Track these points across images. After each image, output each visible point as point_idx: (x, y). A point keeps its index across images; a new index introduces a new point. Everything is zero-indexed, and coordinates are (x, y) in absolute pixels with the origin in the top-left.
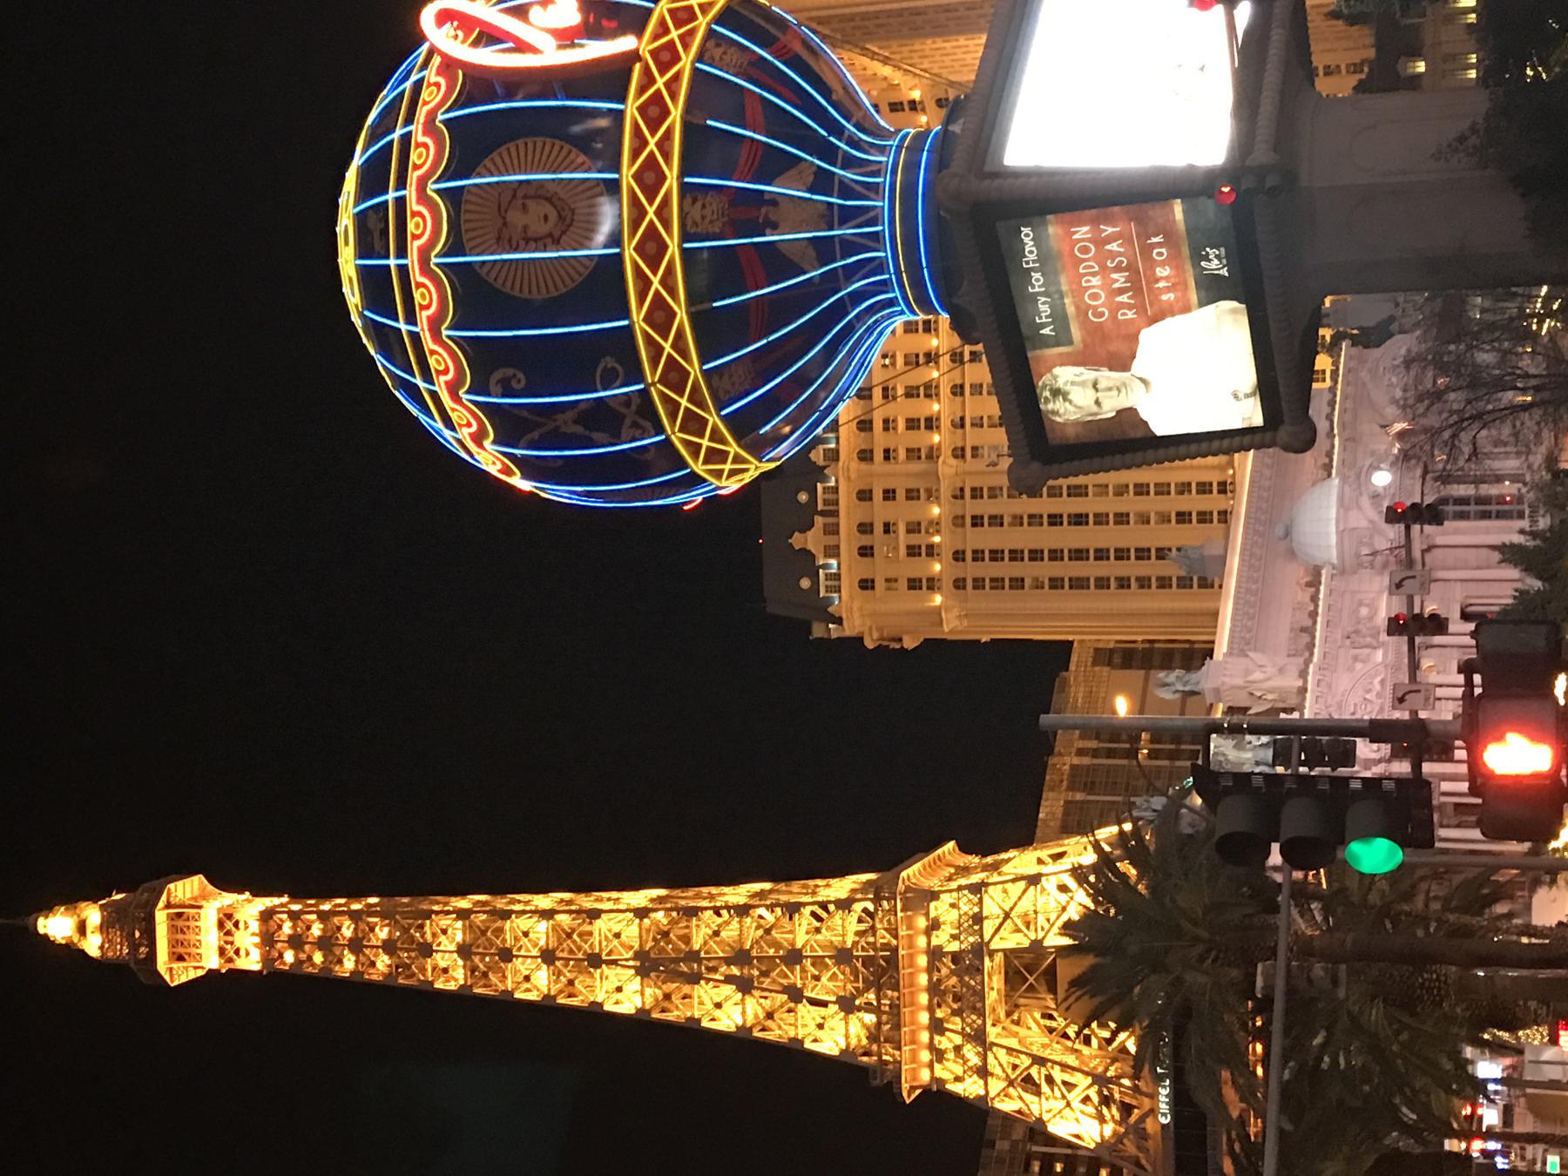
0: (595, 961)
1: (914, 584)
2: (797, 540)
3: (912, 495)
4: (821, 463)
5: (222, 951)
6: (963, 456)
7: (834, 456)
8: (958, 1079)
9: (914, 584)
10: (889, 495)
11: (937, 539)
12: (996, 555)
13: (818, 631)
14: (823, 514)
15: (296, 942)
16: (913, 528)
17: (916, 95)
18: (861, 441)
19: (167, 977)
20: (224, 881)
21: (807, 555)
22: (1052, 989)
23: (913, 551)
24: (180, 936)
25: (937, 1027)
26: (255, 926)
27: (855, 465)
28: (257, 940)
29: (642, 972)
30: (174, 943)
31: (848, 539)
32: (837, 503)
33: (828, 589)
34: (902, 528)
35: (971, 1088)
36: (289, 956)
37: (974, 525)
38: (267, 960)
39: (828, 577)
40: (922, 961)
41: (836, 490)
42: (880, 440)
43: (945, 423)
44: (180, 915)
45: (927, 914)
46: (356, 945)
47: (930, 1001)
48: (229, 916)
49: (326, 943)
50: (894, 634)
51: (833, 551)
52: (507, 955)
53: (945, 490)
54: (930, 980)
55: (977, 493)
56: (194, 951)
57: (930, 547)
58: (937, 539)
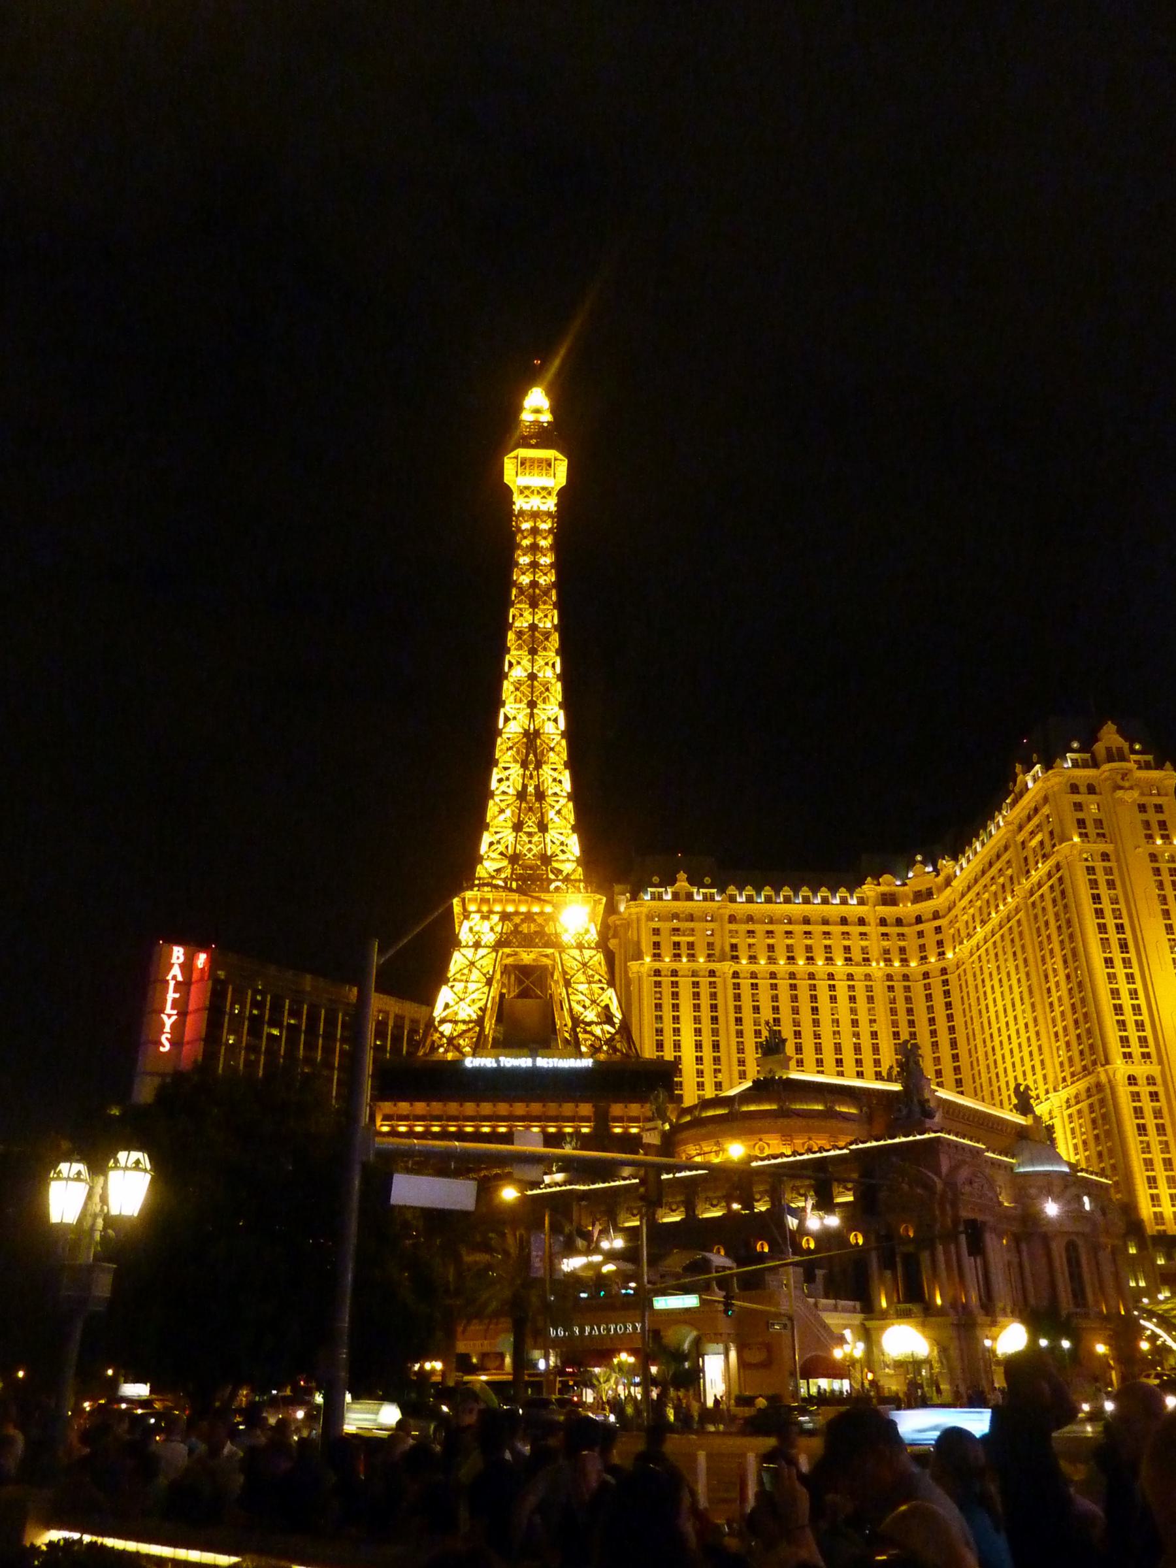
0: (532, 705)
1: (657, 945)
2: (682, 876)
5: (527, 488)
6: (734, 977)
7: (732, 899)
8: (471, 929)
9: (657, 945)
11: (684, 959)
12: (675, 995)
13: (617, 888)
15: (535, 531)
16: (691, 945)
17: (949, 955)
19: (512, 454)
20: (562, 493)
21: (673, 882)
22: (519, 996)
23: (677, 945)
25: (505, 917)
26: (544, 508)
28: (535, 509)
29: (526, 733)
30: (532, 460)
31: (682, 906)
33: (653, 894)
34: (690, 939)
35: (465, 936)
36: (526, 526)
37: (693, 983)
38: (522, 513)
39: (660, 894)
41: (713, 900)
43: (753, 968)
44: (550, 465)
46: (534, 565)
47: (522, 913)
48: (549, 493)
49: (534, 548)
50: (621, 931)
51: (676, 897)
52: (533, 652)
54: (536, 914)
55: (712, 984)
56: (527, 471)
57: (679, 955)
58: (684, 959)
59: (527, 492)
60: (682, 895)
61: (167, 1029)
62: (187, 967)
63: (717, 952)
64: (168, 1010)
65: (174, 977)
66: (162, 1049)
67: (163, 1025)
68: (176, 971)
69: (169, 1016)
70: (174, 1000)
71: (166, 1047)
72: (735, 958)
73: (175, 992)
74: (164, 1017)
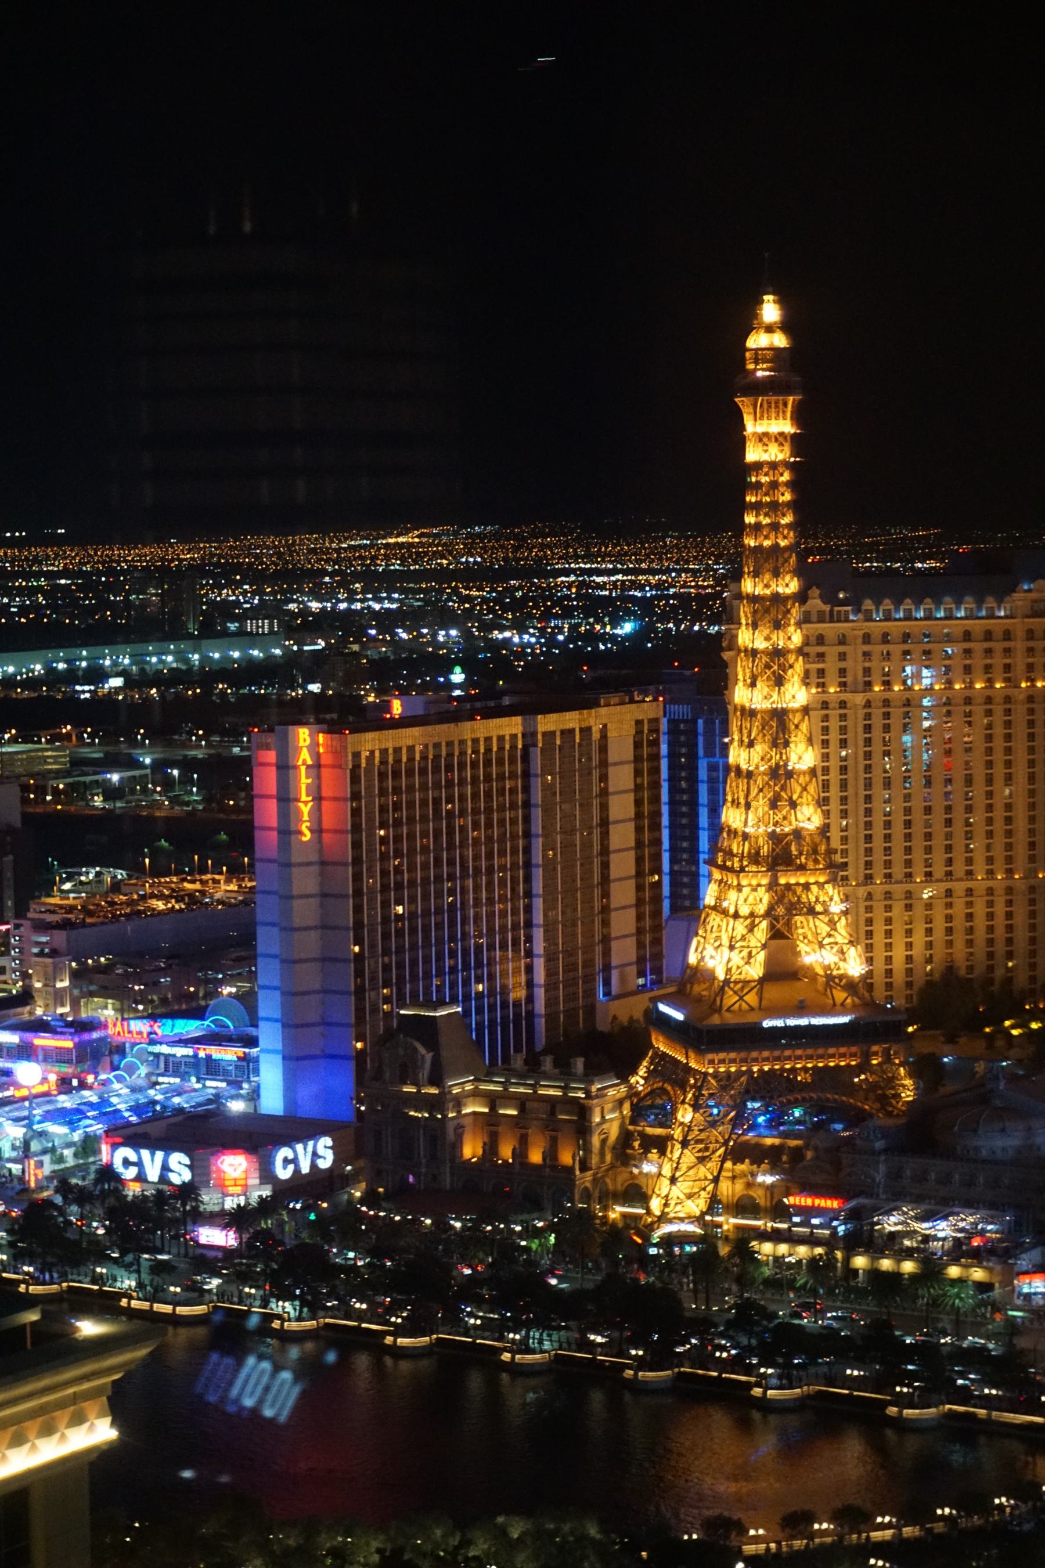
3: (843, 672)
4: (864, 608)
5: (766, 434)
10: (842, 657)
14: (831, 611)
18: (876, 635)
24: (773, 405)
27: (861, 633)
32: (839, 621)
34: (821, 666)
40: (802, 881)
41: (847, 620)
42: (877, 649)
45: (826, 882)
46: (775, 527)
53: (845, 696)
55: (843, 717)
59: (765, 440)
60: (814, 618)
61: (306, 817)
62: (313, 747)
63: (849, 679)
64: (304, 798)
65: (304, 762)
66: (304, 839)
67: (300, 812)
68: (305, 756)
69: (306, 803)
70: (308, 785)
71: (307, 836)
72: (868, 685)
73: (307, 777)
74: (301, 805)
